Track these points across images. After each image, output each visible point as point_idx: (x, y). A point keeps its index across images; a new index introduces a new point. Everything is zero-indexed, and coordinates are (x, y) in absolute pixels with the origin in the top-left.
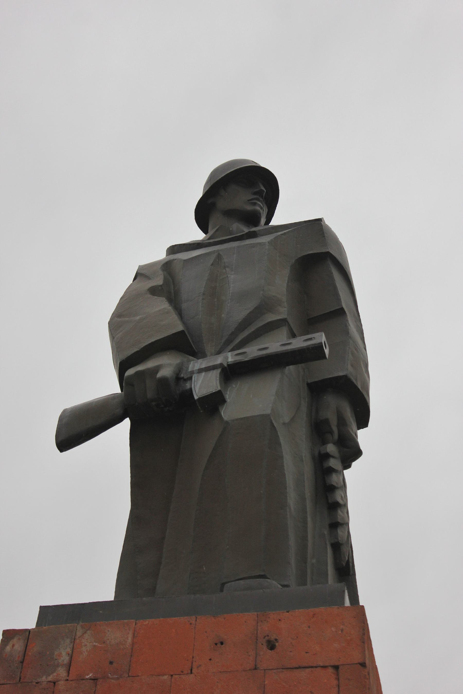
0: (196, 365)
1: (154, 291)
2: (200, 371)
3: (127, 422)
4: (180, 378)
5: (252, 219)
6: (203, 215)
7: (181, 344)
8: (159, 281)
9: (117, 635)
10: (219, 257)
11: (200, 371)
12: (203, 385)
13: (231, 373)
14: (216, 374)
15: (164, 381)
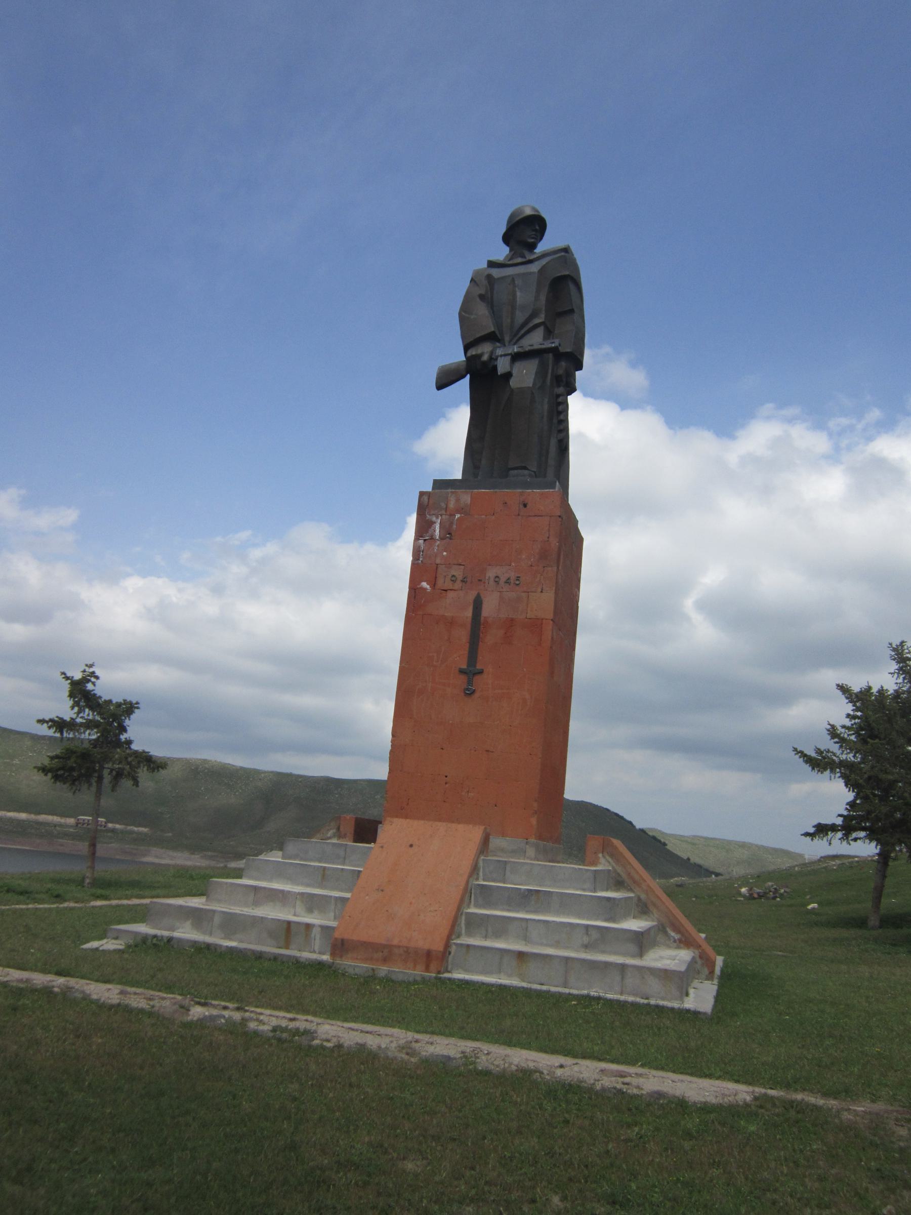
0: (499, 352)
1: (482, 297)
2: (501, 356)
3: (468, 376)
4: (493, 358)
5: (532, 247)
6: (507, 239)
7: (492, 337)
8: (483, 292)
9: (466, 498)
10: (513, 280)
11: (501, 356)
12: (503, 365)
13: (516, 357)
14: (509, 358)
15: (484, 363)
